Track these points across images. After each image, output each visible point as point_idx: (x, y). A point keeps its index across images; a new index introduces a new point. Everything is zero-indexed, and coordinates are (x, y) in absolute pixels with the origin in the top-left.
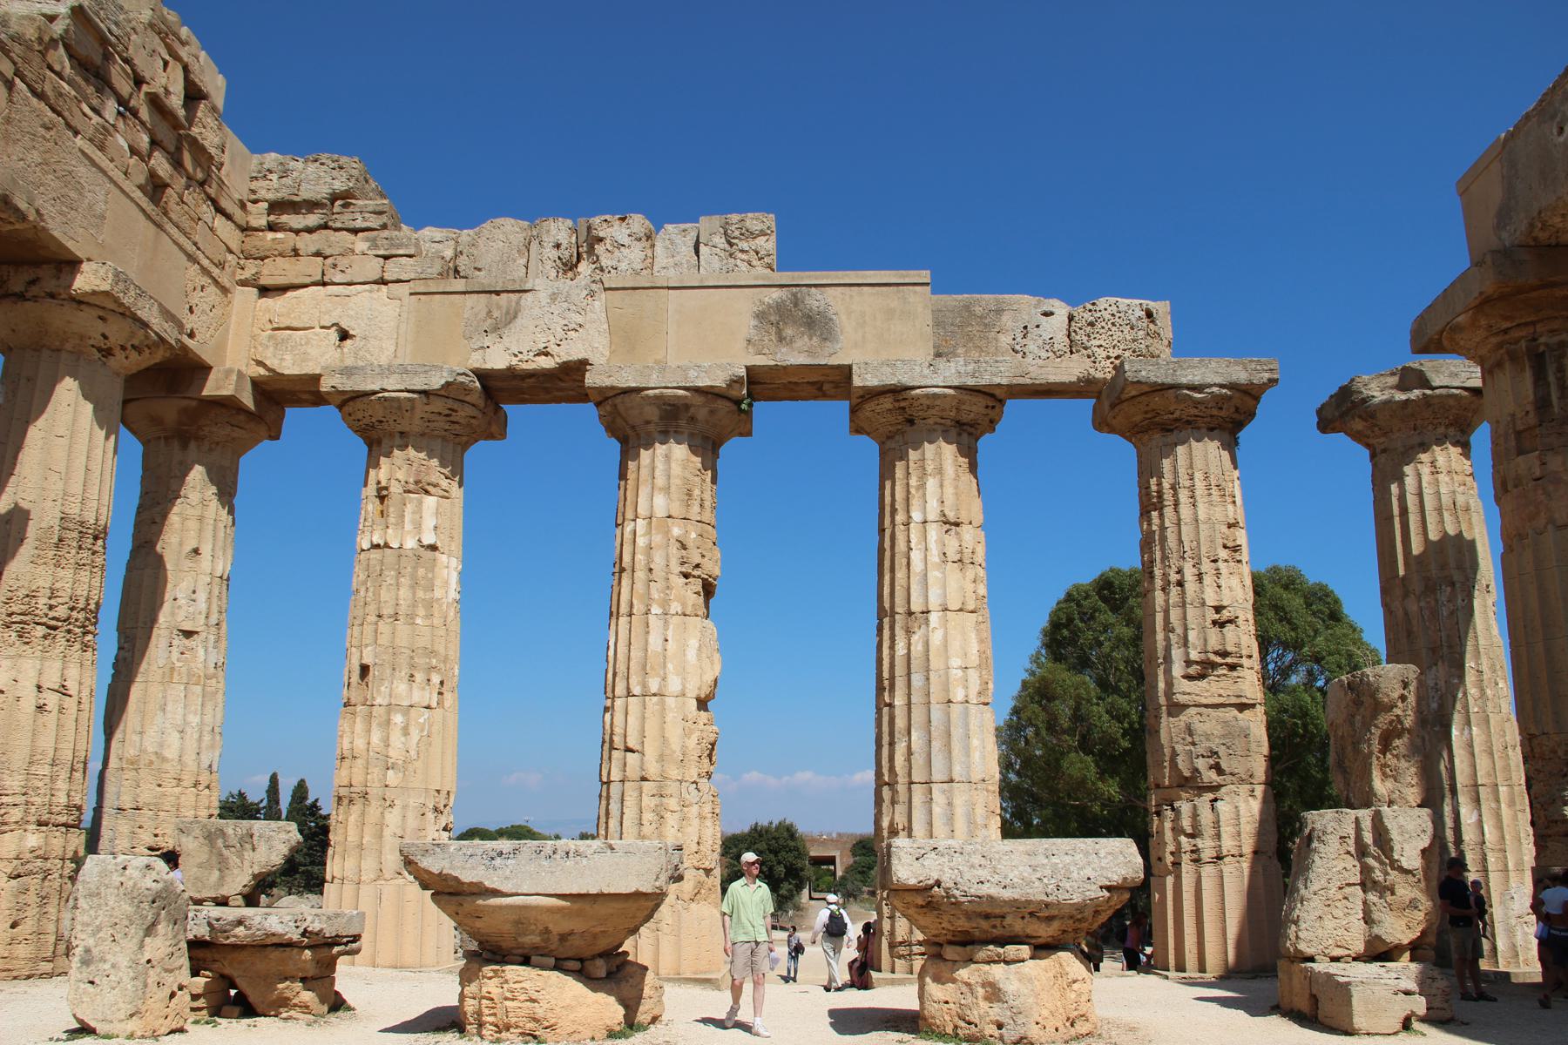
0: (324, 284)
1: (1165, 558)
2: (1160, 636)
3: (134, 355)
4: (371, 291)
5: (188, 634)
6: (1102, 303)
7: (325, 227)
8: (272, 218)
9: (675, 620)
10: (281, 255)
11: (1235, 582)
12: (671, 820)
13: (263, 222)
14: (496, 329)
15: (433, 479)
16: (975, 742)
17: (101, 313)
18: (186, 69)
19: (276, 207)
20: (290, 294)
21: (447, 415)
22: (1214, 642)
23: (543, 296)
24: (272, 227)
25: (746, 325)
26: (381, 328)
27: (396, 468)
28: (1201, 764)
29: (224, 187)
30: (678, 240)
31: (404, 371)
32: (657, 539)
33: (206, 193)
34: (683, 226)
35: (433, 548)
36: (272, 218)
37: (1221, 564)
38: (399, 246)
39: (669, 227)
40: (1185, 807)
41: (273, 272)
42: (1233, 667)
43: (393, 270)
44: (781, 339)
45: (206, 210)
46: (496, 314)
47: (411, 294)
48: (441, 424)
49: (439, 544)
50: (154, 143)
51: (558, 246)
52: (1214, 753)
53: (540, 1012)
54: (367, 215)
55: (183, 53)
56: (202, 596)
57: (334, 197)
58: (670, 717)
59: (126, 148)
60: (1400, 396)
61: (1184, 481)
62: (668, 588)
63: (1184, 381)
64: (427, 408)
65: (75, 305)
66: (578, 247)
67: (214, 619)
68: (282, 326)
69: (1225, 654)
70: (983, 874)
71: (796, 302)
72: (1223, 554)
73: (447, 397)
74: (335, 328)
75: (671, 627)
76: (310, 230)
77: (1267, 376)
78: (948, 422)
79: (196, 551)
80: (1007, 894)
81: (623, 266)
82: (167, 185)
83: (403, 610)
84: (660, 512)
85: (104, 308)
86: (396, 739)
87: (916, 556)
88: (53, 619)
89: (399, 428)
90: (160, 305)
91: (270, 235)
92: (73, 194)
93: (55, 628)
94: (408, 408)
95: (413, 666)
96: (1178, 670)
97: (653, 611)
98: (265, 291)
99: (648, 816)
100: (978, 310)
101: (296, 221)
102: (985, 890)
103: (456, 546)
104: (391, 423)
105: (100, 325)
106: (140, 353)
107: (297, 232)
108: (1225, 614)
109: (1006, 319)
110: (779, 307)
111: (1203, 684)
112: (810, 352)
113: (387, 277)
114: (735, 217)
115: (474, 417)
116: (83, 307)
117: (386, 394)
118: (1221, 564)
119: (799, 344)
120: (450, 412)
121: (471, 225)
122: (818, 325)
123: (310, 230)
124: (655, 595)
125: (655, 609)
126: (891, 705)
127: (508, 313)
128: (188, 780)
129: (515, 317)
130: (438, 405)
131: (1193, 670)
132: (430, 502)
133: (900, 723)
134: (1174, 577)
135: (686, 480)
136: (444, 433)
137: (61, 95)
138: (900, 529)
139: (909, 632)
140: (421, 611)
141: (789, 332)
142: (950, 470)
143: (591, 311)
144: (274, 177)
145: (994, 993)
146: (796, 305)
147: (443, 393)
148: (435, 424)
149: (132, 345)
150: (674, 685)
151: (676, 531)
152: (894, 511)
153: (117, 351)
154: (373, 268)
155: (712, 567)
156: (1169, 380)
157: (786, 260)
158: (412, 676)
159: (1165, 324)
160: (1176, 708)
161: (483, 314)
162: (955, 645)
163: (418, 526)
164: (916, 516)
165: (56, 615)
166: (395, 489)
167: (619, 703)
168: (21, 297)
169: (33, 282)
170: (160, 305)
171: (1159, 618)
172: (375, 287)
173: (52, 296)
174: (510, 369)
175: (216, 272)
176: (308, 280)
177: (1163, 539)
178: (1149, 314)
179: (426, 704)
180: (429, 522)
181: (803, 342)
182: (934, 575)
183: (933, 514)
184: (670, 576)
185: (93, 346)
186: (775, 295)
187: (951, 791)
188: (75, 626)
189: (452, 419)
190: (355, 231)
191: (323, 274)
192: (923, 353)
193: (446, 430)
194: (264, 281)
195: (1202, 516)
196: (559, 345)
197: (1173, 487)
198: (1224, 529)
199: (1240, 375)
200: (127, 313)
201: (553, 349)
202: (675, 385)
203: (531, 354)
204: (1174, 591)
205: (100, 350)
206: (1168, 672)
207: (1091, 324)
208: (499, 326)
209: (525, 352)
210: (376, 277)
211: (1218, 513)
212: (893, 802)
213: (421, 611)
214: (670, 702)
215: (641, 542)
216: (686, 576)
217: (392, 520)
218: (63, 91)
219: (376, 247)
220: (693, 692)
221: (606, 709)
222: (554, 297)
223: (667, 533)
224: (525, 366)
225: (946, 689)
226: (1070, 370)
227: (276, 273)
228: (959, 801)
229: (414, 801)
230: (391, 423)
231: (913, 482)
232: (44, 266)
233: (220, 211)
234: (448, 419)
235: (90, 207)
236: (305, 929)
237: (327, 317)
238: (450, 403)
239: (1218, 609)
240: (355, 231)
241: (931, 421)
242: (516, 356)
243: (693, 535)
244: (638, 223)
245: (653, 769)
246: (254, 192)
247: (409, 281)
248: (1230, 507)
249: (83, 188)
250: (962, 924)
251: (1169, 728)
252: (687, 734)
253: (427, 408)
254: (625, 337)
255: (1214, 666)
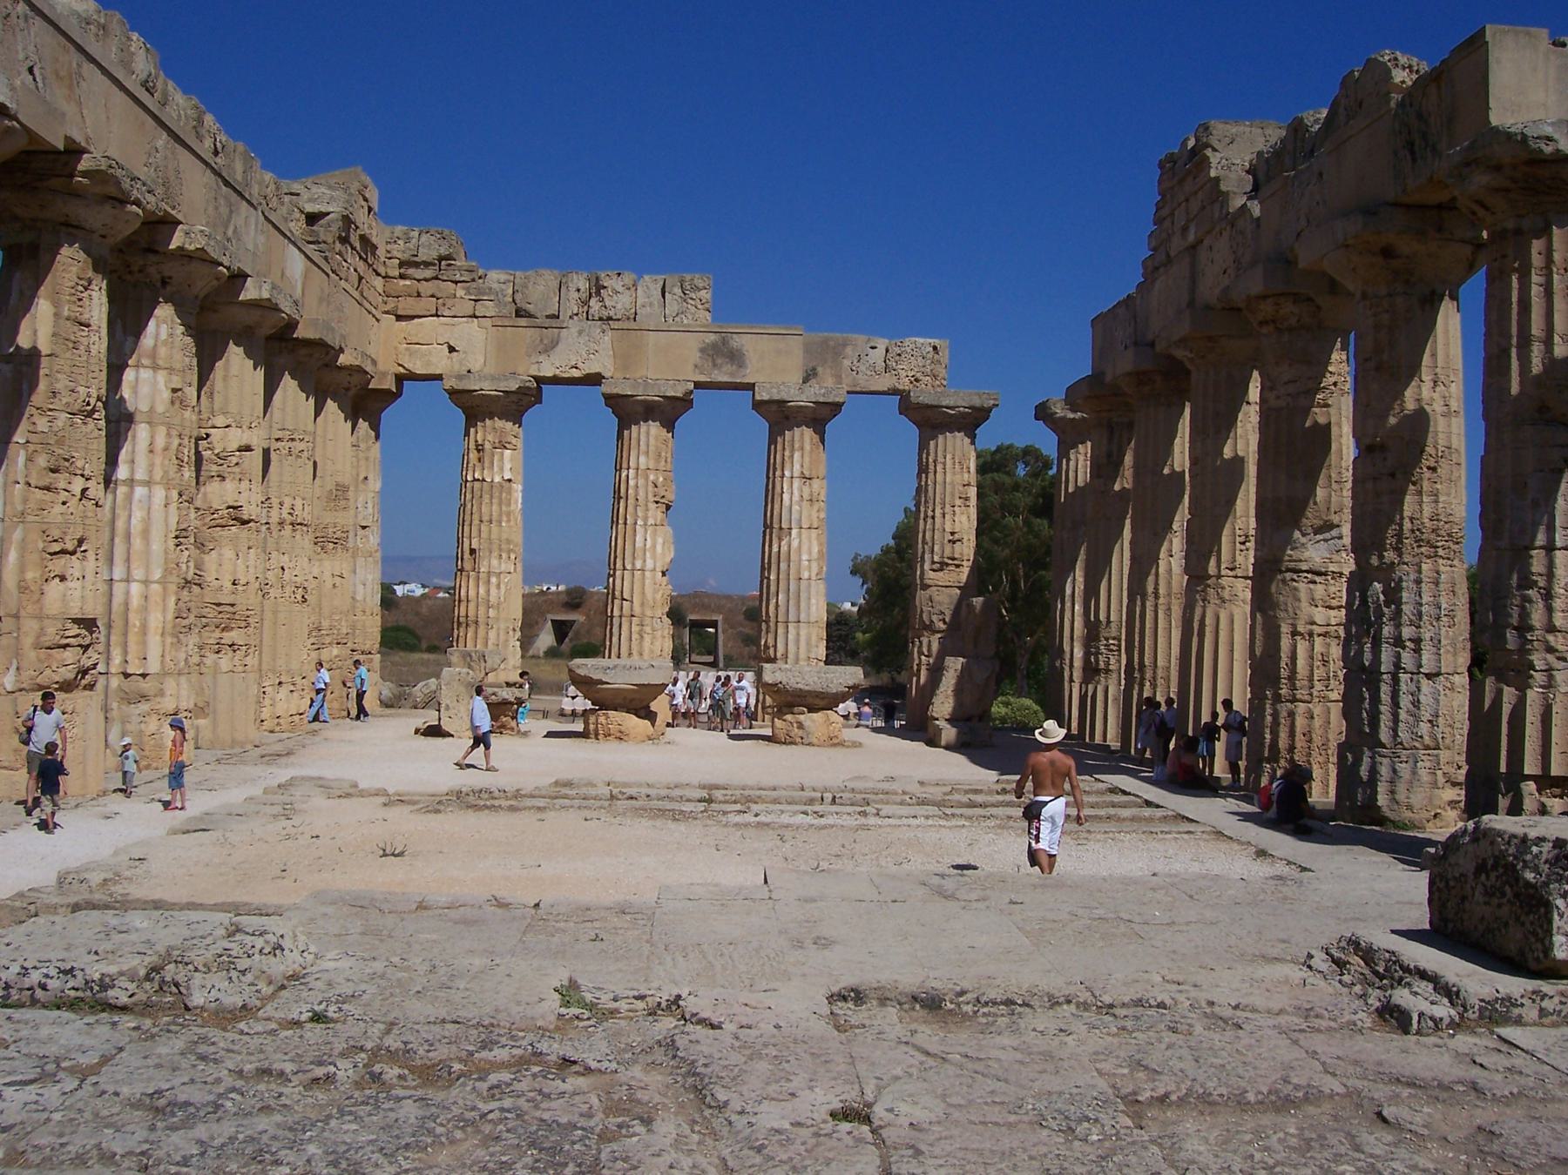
0: (438, 316)
1: (926, 502)
2: (920, 546)
5: (364, 527)
6: (907, 341)
7: (436, 278)
8: (402, 271)
11: (964, 518)
12: (647, 638)
13: (396, 273)
14: (546, 351)
16: (813, 601)
19: (402, 264)
20: (416, 320)
22: (947, 553)
23: (574, 331)
24: (402, 277)
25: (695, 356)
27: (487, 432)
28: (934, 618)
30: (652, 286)
32: (641, 482)
34: (655, 277)
35: (510, 480)
36: (402, 271)
37: (956, 509)
38: (484, 294)
39: (647, 277)
40: (925, 640)
41: (406, 306)
42: (958, 566)
44: (715, 365)
51: (578, 290)
52: (943, 613)
53: (623, 728)
56: (370, 505)
57: (441, 259)
58: (647, 582)
60: (1071, 415)
61: (940, 459)
63: (944, 404)
69: (953, 559)
70: (798, 680)
71: (724, 342)
72: (958, 502)
76: (426, 280)
77: (992, 402)
79: (366, 478)
80: (807, 688)
81: (619, 306)
84: (642, 467)
86: (493, 591)
87: (786, 497)
91: (402, 282)
95: (500, 550)
96: (927, 566)
98: (399, 318)
99: (635, 636)
100: (832, 343)
102: (800, 686)
103: (520, 478)
107: (419, 281)
108: (956, 537)
109: (849, 350)
110: (714, 345)
111: (940, 574)
112: (732, 374)
113: (477, 314)
114: (688, 277)
118: (956, 509)
119: (724, 369)
121: (525, 268)
122: (736, 357)
123: (426, 280)
124: (640, 514)
125: (640, 522)
126: (768, 578)
128: (368, 613)
130: (514, 398)
131: (936, 566)
132: (507, 452)
133: (773, 588)
134: (930, 513)
135: (657, 447)
138: (778, 480)
139: (780, 540)
140: (505, 518)
141: (719, 361)
142: (807, 447)
145: (801, 726)
150: (649, 564)
151: (652, 477)
152: (775, 469)
154: (468, 308)
155: (670, 496)
156: (935, 403)
157: (718, 310)
159: (944, 355)
160: (925, 587)
161: (538, 341)
162: (805, 548)
163: (502, 469)
164: (787, 473)
166: (488, 446)
167: (618, 573)
171: (920, 536)
175: (374, 311)
177: (927, 491)
178: (935, 348)
180: (507, 466)
181: (728, 368)
182: (796, 508)
183: (796, 474)
186: (712, 337)
187: (798, 627)
190: (456, 282)
192: (797, 377)
194: (399, 313)
195: (948, 480)
197: (935, 461)
198: (961, 488)
199: (977, 402)
201: (580, 365)
204: (930, 521)
206: (922, 566)
208: (549, 348)
211: (958, 478)
212: (767, 632)
213: (505, 518)
214: (648, 574)
215: (632, 483)
216: (657, 502)
217: (486, 465)
220: (659, 569)
221: (609, 575)
222: (580, 333)
223: (647, 478)
225: (799, 573)
226: (884, 383)
228: (803, 633)
229: (502, 626)
231: (787, 453)
239: (952, 534)
240: (456, 282)
244: (628, 278)
246: (389, 252)
248: (966, 475)
250: (789, 698)
251: (921, 596)
252: (655, 591)
254: (625, 359)
255: (947, 565)
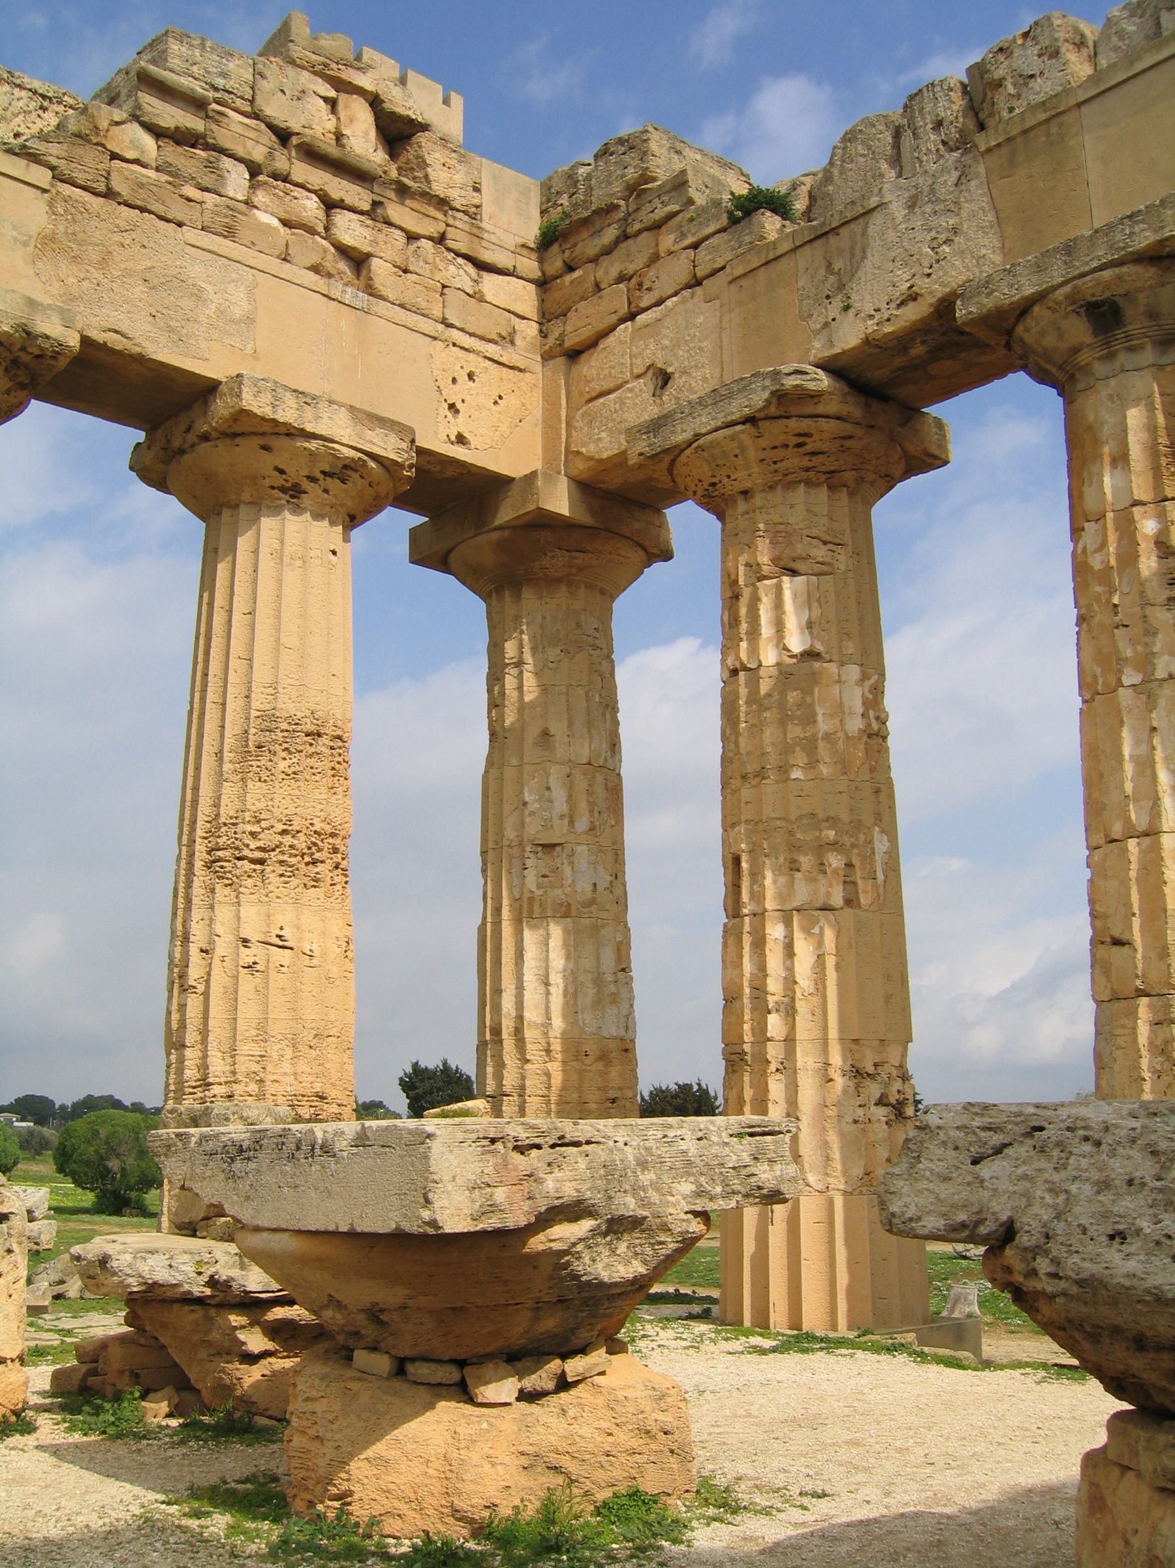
3: (334, 484)
4: (684, 301)
7: (625, 237)
10: (583, 298)
15: (800, 549)
18: (375, 102)
21: (799, 445)
23: (898, 209)
26: (701, 349)
29: (486, 236)
31: (717, 396)
33: (449, 250)
43: (706, 260)
45: (461, 275)
47: (730, 282)
48: (794, 461)
49: (819, 647)
50: (330, 205)
54: (665, 198)
55: (364, 81)
59: (275, 223)
62: (1147, 633)
64: (762, 443)
65: (228, 441)
66: (977, 114)
67: (582, 824)
68: (594, 394)
73: (788, 418)
74: (650, 373)
75: (1162, 702)
76: (608, 251)
82: (369, 256)
83: (773, 760)
85: (263, 434)
88: (259, 849)
90: (352, 409)
91: (568, 278)
92: (186, 303)
93: (261, 862)
94: (737, 451)
97: (1126, 681)
101: (590, 246)
104: (725, 481)
106: (343, 481)
107: (595, 260)
115: (850, 437)
116: (238, 440)
117: (701, 441)
120: (801, 440)
123: (608, 251)
125: (1131, 677)
129: (864, 257)
136: (805, 475)
137: (141, 185)
143: (967, 201)
147: (773, 410)
148: (786, 464)
149: (323, 472)
153: (306, 485)
158: (794, 861)
165: (261, 844)
168: (182, 452)
169: (189, 429)
170: (352, 409)
172: (687, 293)
173: (205, 438)
174: (867, 341)
176: (614, 318)
179: (819, 904)
184: (1149, 611)
185: (273, 488)
188: (291, 856)
189: (809, 448)
191: (630, 303)
193: (807, 470)
194: (568, 344)
196: (929, 275)
200: (294, 431)
201: (922, 284)
202: (1095, 264)
203: (893, 305)
205: (283, 490)
209: (884, 306)
210: (684, 277)
213: (800, 758)
218: (144, 180)
224: (888, 329)
227: (580, 324)
230: (725, 481)
232: (195, 405)
233: (483, 267)
234: (801, 450)
235: (220, 312)
236: (212, 1277)
237: (639, 361)
242: (871, 317)
247: (723, 268)
249: (201, 289)
253: (762, 443)
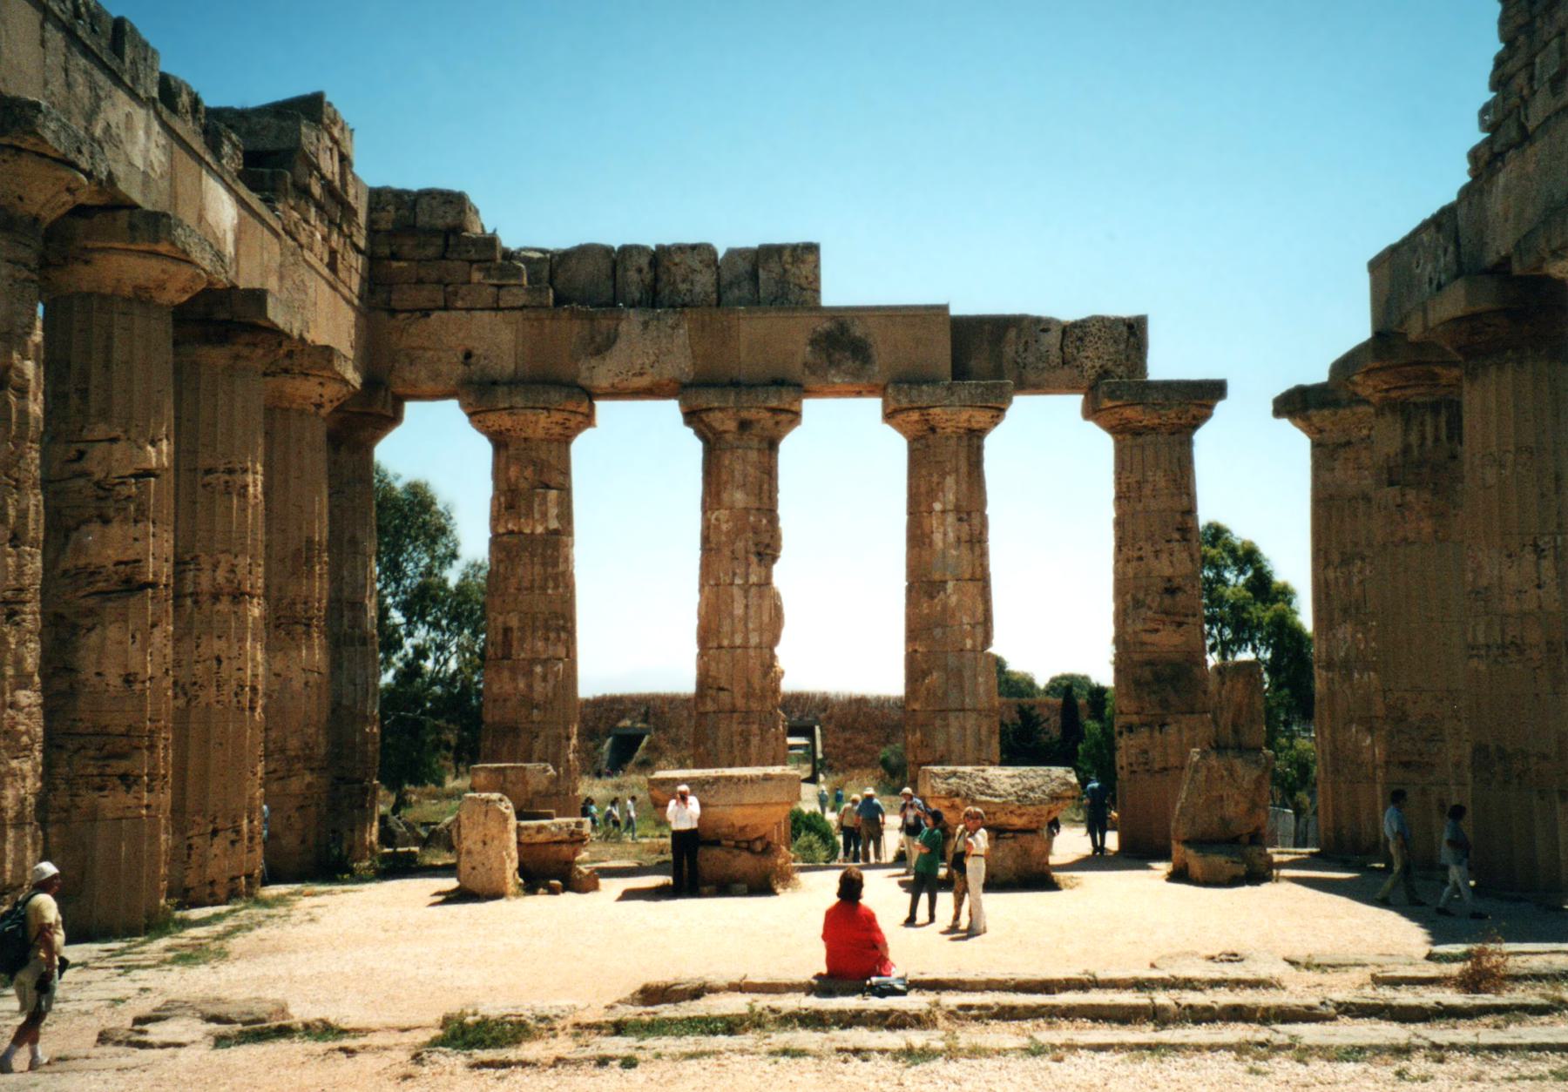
9: (753, 590)
17: (321, 380)
46: (598, 339)
78: (962, 431)
86: (539, 687)
89: (523, 435)
105: (319, 390)
127: (608, 337)
140: (551, 584)
144: (390, 208)
146: (842, 334)
163: (544, 515)
207: (1081, 339)
213: (551, 584)
214: (752, 652)
219: (490, 276)
238: (566, 415)
241: (949, 430)
243: (764, 521)
245: (740, 703)
